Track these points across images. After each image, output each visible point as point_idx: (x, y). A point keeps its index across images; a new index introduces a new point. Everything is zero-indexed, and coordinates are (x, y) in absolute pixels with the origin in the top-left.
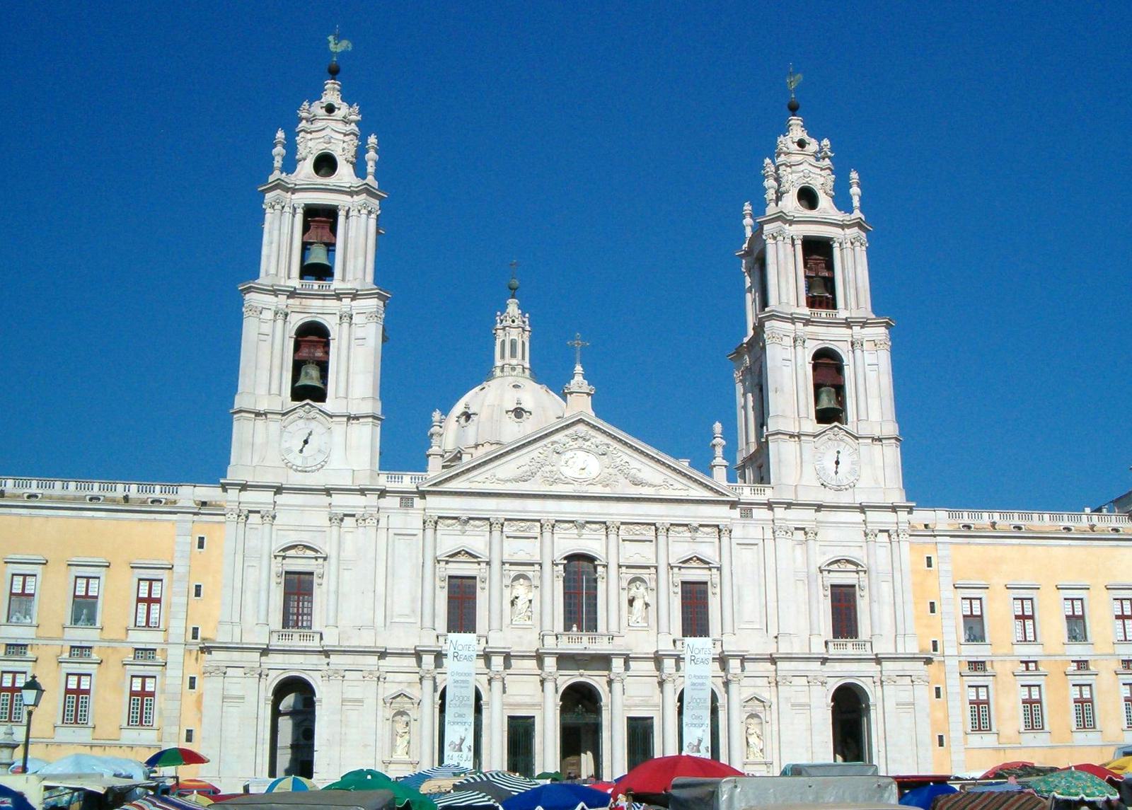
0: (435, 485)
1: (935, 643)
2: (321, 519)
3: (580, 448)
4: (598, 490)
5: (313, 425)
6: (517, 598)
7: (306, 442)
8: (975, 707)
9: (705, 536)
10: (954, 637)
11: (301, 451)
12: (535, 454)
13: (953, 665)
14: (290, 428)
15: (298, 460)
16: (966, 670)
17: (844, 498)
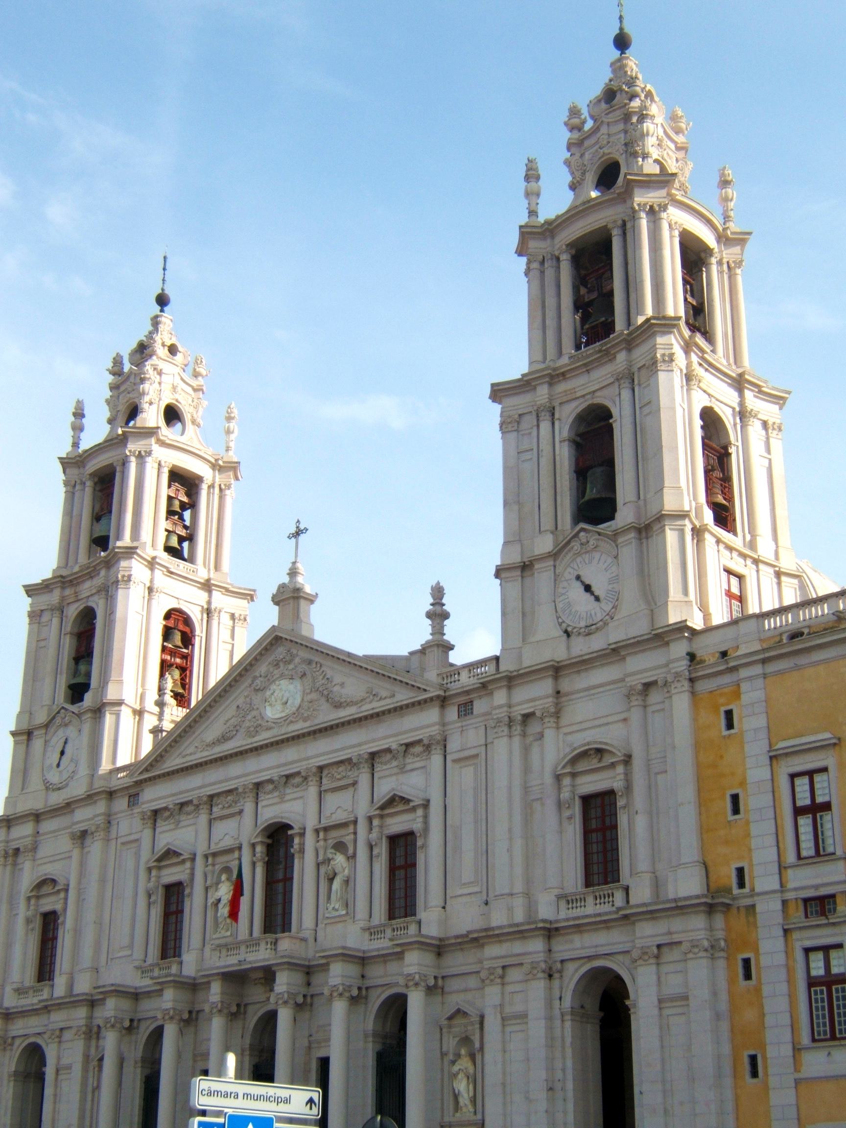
0: (146, 770)
1: (740, 871)
2: (64, 843)
3: (282, 676)
4: (300, 726)
5: (71, 732)
6: (219, 900)
7: (62, 753)
8: (822, 992)
9: (416, 759)
10: (771, 854)
11: (58, 765)
12: (240, 701)
13: (769, 910)
14: (54, 740)
15: (54, 777)
16: (797, 914)
17: (597, 643)
